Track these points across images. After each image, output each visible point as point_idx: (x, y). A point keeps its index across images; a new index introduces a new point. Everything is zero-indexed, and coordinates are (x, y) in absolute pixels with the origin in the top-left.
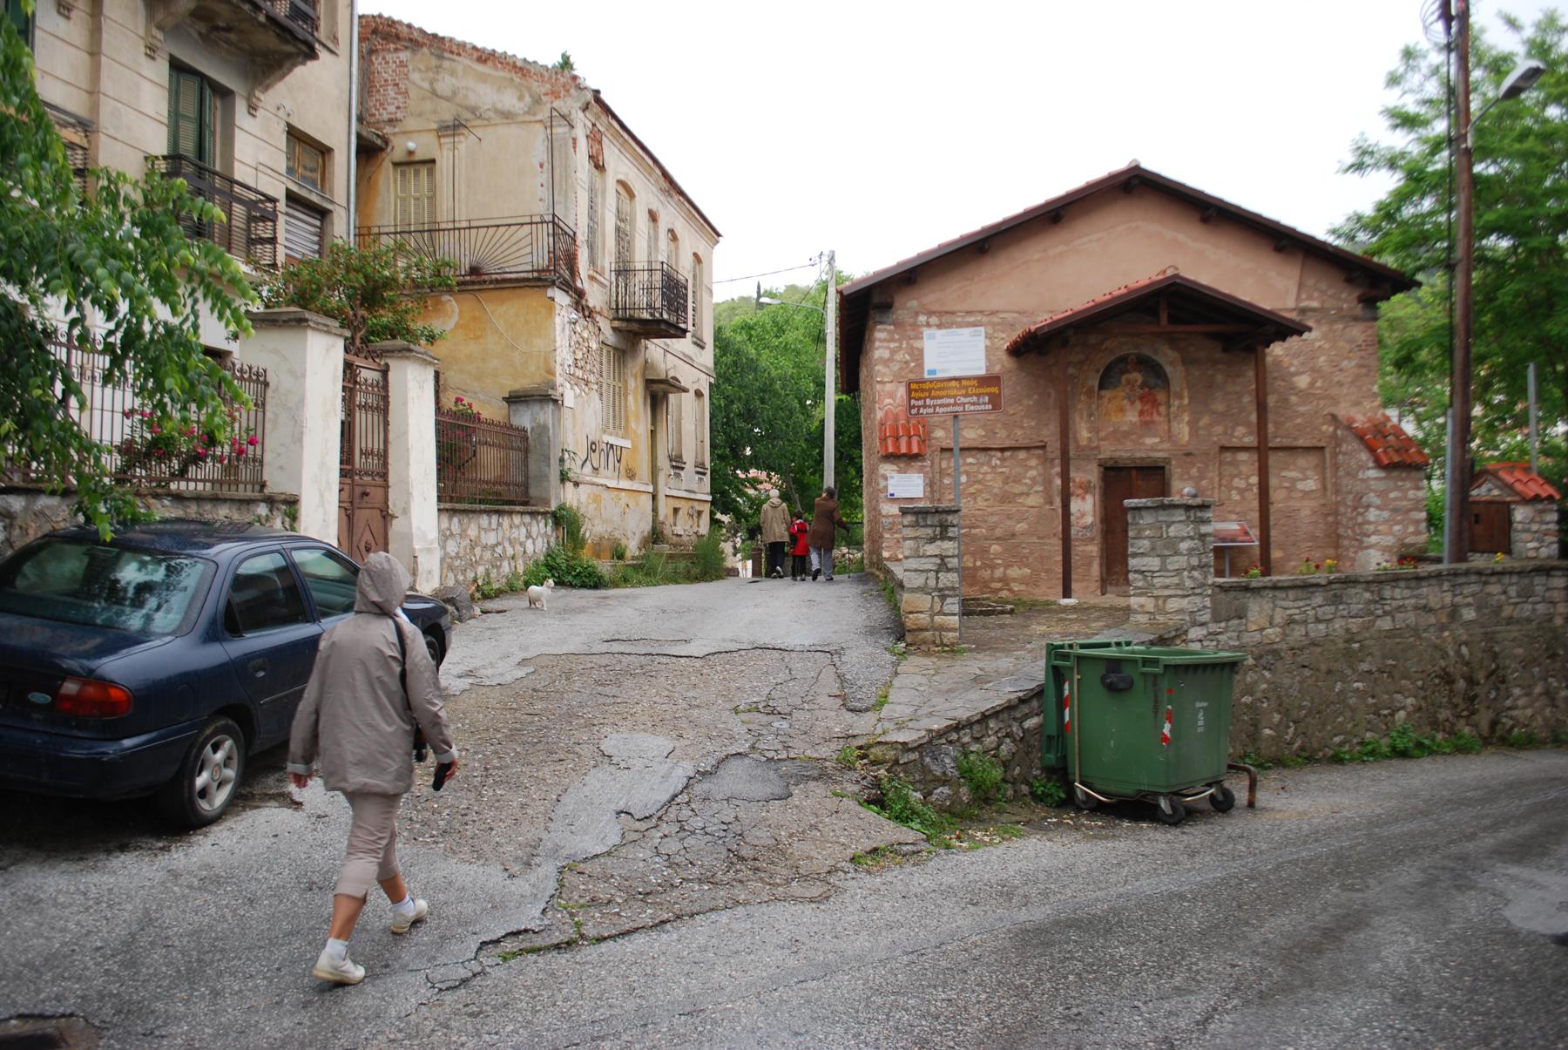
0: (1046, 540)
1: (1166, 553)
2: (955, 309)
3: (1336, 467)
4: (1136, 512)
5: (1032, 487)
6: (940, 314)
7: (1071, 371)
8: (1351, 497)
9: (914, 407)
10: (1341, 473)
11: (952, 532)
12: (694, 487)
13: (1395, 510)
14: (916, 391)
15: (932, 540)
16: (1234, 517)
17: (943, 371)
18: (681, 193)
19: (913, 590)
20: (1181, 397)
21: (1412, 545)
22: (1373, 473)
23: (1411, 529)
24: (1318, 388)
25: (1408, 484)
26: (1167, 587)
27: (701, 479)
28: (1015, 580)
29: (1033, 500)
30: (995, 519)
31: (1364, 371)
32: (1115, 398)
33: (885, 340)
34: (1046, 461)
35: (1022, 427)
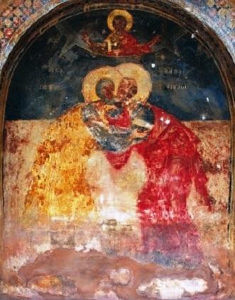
32: (58, 146)
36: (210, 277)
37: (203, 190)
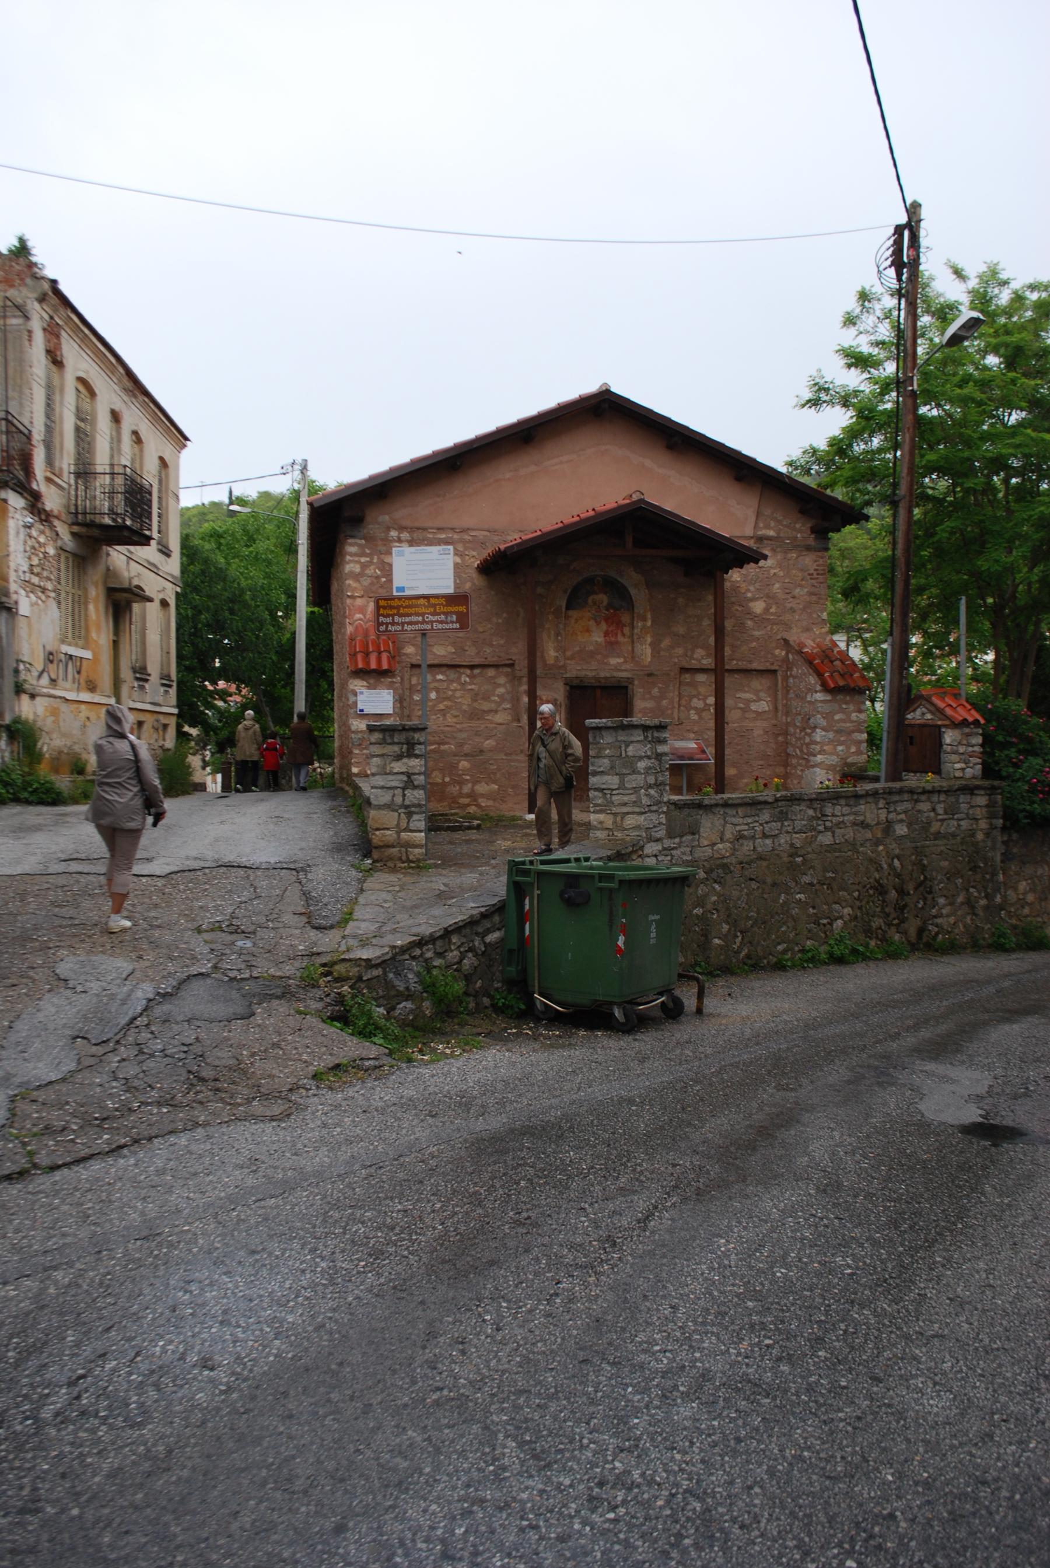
0: (514, 757)
1: (625, 771)
2: (427, 524)
3: (787, 689)
4: (597, 732)
5: (499, 704)
6: (411, 530)
7: (540, 590)
8: (799, 718)
9: (382, 624)
10: (791, 695)
11: (419, 749)
12: (160, 699)
13: (839, 732)
14: (384, 608)
15: (399, 757)
16: (692, 735)
17: (412, 588)
18: (146, 393)
19: (380, 807)
20: (644, 619)
21: (853, 764)
22: (820, 696)
23: (853, 749)
24: (772, 614)
25: (851, 707)
26: (625, 804)
27: (166, 692)
28: (482, 795)
29: (500, 718)
30: (464, 735)
31: (814, 598)
33: (356, 555)
34: (514, 679)
35: (491, 645)
36: (625, 658)
37: (622, 632)
